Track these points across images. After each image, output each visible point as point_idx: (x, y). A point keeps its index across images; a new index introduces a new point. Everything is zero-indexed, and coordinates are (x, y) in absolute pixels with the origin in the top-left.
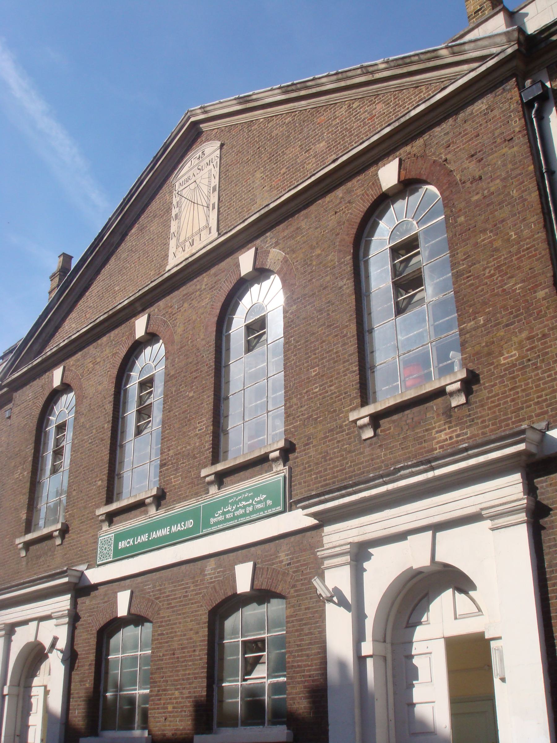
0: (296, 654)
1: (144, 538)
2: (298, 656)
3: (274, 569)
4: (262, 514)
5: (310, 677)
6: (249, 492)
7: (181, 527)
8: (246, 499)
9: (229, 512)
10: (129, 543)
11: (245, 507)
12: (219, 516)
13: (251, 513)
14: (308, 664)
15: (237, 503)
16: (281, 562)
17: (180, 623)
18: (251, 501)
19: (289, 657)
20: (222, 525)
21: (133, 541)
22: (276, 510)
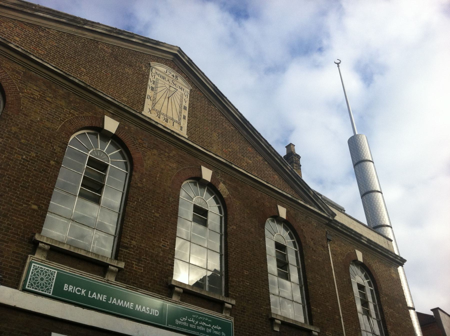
1: (103, 298)
6: (209, 318)
8: (207, 322)
9: (191, 323)
10: (81, 291)
11: (204, 326)
12: (184, 321)
15: (200, 320)
18: (210, 325)
20: (186, 330)
21: (87, 293)
22: (190, 332)
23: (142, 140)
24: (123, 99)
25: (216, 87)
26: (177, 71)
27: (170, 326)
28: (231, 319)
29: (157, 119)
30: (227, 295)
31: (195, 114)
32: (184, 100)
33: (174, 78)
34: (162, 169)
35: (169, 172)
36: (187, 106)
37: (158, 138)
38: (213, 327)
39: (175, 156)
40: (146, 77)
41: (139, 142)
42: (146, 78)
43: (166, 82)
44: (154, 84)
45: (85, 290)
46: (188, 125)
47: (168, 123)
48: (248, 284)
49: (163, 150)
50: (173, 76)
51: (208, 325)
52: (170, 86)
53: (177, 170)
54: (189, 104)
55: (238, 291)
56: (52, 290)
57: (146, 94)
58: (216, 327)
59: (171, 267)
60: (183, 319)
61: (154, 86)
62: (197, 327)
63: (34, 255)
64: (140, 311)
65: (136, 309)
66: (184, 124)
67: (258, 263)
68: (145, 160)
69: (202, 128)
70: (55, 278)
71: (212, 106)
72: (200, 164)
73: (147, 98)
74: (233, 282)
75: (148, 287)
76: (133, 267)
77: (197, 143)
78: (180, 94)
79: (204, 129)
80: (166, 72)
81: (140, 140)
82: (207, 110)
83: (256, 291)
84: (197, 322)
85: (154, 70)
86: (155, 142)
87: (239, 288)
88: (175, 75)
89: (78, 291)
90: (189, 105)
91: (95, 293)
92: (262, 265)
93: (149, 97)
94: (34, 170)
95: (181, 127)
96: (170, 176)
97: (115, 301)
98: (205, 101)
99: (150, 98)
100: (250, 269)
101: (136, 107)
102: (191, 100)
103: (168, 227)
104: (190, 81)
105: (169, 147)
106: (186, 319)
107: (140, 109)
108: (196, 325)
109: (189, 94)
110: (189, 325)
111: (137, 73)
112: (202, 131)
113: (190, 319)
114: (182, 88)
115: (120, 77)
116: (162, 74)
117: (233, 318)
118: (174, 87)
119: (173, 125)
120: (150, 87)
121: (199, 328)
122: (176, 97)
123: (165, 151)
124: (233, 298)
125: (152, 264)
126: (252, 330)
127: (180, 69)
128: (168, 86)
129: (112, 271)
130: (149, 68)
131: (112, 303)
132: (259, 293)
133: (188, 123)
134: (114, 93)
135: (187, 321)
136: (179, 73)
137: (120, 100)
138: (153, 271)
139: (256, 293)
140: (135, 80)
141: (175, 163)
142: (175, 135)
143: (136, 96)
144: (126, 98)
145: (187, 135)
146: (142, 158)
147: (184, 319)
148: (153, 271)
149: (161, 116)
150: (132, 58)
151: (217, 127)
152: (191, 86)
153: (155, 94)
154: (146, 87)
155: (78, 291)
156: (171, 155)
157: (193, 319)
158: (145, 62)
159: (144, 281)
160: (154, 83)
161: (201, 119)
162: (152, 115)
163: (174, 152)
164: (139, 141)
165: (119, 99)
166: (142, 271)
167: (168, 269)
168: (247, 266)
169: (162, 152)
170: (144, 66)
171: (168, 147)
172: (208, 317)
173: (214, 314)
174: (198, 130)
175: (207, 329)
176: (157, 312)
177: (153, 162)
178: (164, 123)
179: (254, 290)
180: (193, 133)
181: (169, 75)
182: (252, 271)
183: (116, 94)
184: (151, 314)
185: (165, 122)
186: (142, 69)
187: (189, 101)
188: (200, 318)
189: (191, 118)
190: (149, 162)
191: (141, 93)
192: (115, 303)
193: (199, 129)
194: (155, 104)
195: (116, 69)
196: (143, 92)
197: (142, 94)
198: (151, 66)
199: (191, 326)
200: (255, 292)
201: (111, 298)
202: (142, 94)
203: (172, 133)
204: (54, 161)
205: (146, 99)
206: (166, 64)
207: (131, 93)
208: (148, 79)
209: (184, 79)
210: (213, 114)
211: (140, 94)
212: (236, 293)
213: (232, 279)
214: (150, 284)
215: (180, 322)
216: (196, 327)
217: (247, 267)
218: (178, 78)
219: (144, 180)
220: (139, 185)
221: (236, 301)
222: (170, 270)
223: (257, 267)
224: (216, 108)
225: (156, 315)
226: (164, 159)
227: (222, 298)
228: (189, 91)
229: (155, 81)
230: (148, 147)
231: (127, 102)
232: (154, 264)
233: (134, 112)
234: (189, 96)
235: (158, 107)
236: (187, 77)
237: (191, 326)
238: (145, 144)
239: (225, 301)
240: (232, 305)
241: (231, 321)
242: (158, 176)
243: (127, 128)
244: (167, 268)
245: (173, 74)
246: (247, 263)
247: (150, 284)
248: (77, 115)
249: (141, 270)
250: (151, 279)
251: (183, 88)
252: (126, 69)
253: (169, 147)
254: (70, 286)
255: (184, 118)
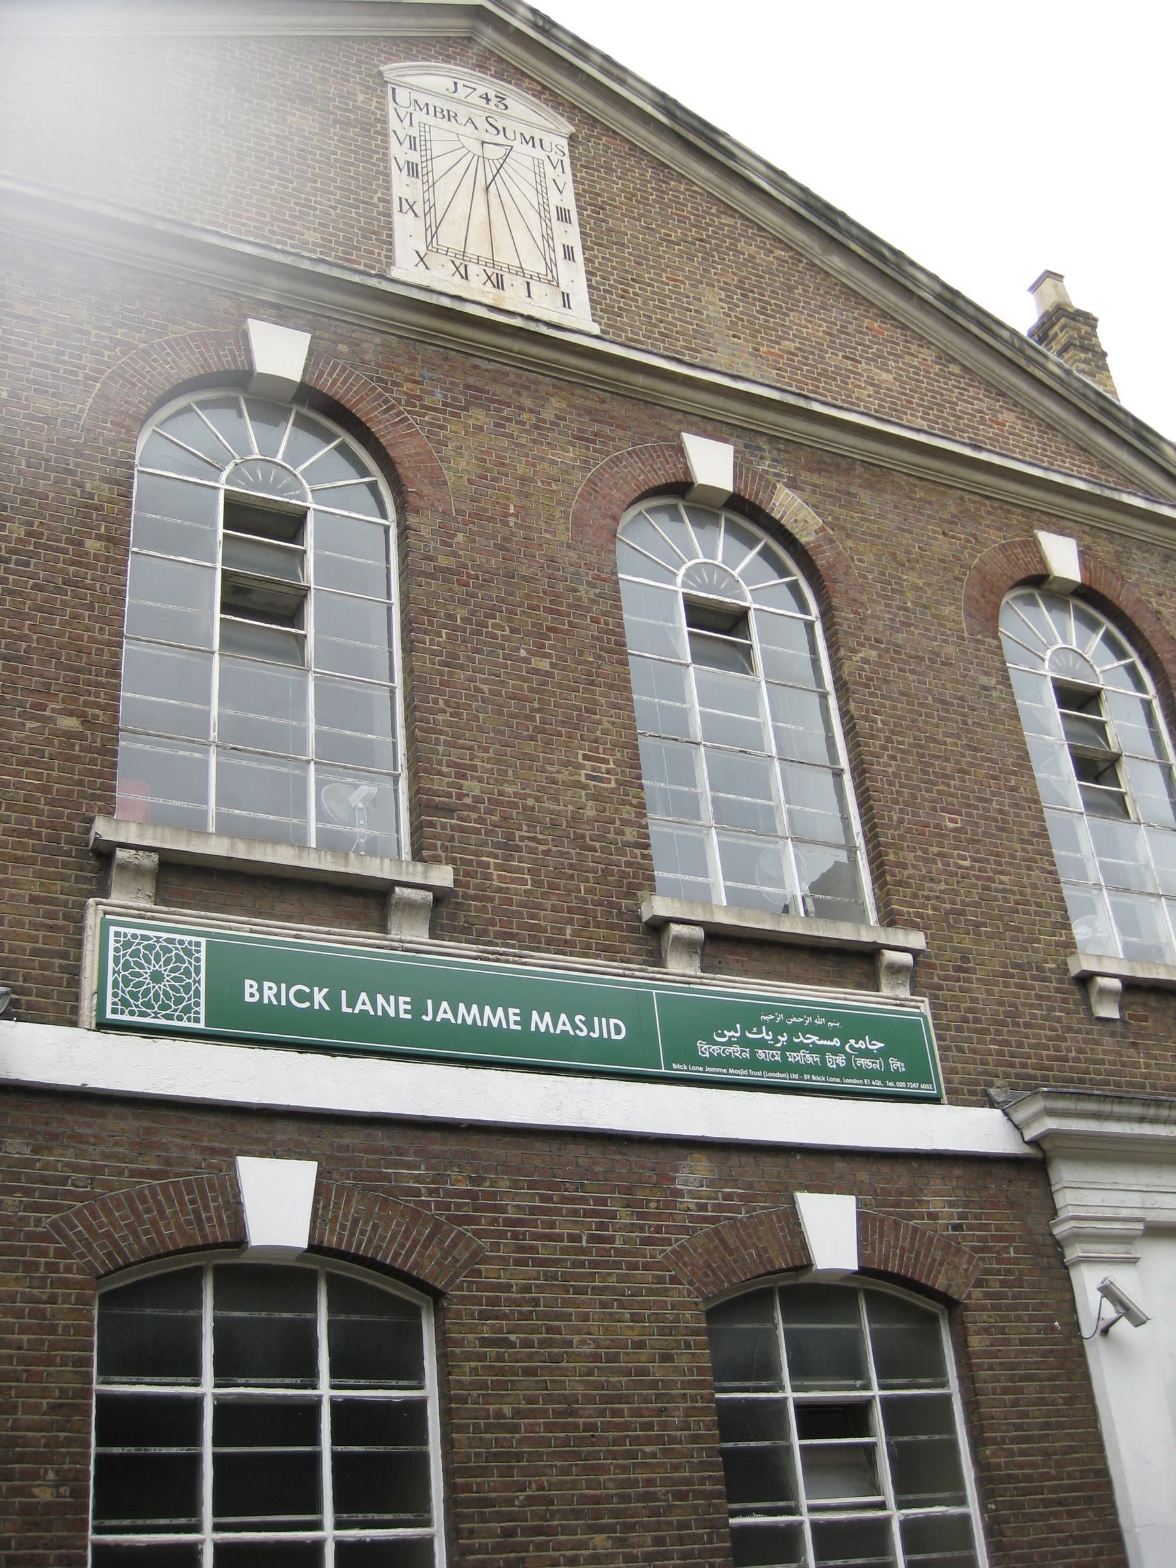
0: (1015, 1447)
1: (398, 1007)
2: (1022, 1453)
3: (915, 1229)
4: (834, 1082)
5: (1060, 1504)
6: (830, 1017)
7: (575, 1027)
8: (824, 1033)
9: (763, 1044)
10: (310, 997)
11: (815, 1049)
12: (729, 1043)
13: (839, 1072)
14: (1048, 1473)
15: (794, 1031)
16: (933, 1216)
17: (585, 1318)
18: (836, 1042)
19: (994, 1454)
23: (415, 382)
24: (305, 237)
25: (675, 102)
26: (499, 76)
27: (678, 1069)
28: (919, 1004)
29: (456, 286)
30: (889, 919)
31: (610, 230)
32: (551, 185)
33: (492, 106)
34: (523, 479)
35: (554, 487)
36: (569, 203)
37: (478, 362)
38: (851, 1047)
39: (564, 419)
40: (379, 128)
41: (406, 394)
42: (376, 132)
43: (462, 130)
44: (415, 150)
45: (325, 990)
46: (588, 280)
47: (508, 292)
48: (967, 863)
49: (509, 405)
50: (488, 100)
51: (829, 1043)
52: (483, 142)
53: (585, 469)
54: (576, 194)
55: (928, 898)
56: (202, 1009)
57: (391, 195)
58: (861, 1045)
59: (638, 852)
60: (725, 1036)
61: (415, 157)
62: (788, 1053)
63: (106, 895)
64: (552, 1031)
65: (533, 1029)
66: (574, 278)
67: (995, 778)
68: (445, 460)
69: (652, 279)
70: (203, 964)
71: (672, 183)
72: (677, 428)
73: (401, 211)
74: (904, 866)
75: (566, 941)
76: (488, 877)
77: (644, 347)
78: (529, 162)
79: (662, 282)
80: (456, 91)
81: (409, 385)
82: (658, 202)
83: (1002, 883)
84: (783, 1039)
85: (402, 95)
86: (471, 380)
87: (930, 885)
88: (491, 95)
89: (300, 996)
90: (577, 200)
91: (363, 996)
92: (1013, 783)
93: (405, 207)
94: (36, 587)
95: (565, 298)
96: (559, 503)
97: (445, 1012)
98: (640, 169)
99: (411, 207)
100: (969, 806)
101: (363, 257)
102: (582, 177)
103: (595, 702)
104: (563, 105)
105: (533, 387)
106: (737, 1032)
107: (379, 261)
108: (783, 1049)
109: (567, 154)
110: (753, 1054)
111: (336, 122)
112: (653, 293)
113: (755, 1030)
114: (532, 138)
115: (272, 155)
116: (440, 104)
117: (926, 999)
118: (500, 139)
119: (529, 296)
120: (401, 164)
121: (792, 1057)
122: (517, 179)
123: (516, 407)
124: (914, 926)
125: (562, 854)
126: (1009, 1032)
127: (508, 62)
128: (476, 148)
129: (410, 906)
130: (381, 91)
131: (438, 1020)
132: (1014, 888)
133: (587, 272)
134: (265, 223)
135: (743, 1042)
136: (510, 82)
137: (293, 246)
138: (571, 877)
139: (1004, 891)
140: (335, 153)
141: (571, 443)
142: (544, 330)
143: (353, 215)
144: (315, 230)
145: (594, 321)
146: (430, 452)
147: (732, 1033)
148: (571, 877)
149: (473, 269)
150: (305, 67)
151: (713, 262)
152: (570, 120)
153: (426, 187)
154: (385, 168)
155: (300, 996)
156: (548, 414)
157: (764, 1027)
158: (360, 73)
159: (542, 923)
160: (413, 146)
161: (639, 245)
162: (433, 273)
163: (554, 402)
164: (405, 389)
165: (289, 241)
166: (529, 887)
167: (629, 864)
168: (952, 795)
169: (506, 412)
170: (358, 88)
171: (527, 388)
172: (823, 1014)
173: (845, 999)
174: (635, 294)
175: (828, 1056)
176: (617, 1028)
177: (477, 458)
178: (489, 295)
179: (994, 882)
180: (620, 308)
181: (469, 99)
182: (975, 812)
183: (273, 225)
184: (595, 1035)
185: (494, 290)
186: (356, 101)
187: (574, 181)
188: (795, 1020)
189: (596, 252)
190: (462, 464)
191: (372, 198)
192: (449, 1020)
193: (640, 289)
194: (437, 228)
195: (252, 125)
196: (376, 192)
197: (375, 200)
198: (387, 82)
199: (761, 1054)
200: (1001, 886)
201: (430, 1002)
202: (375, 200)
203: (532, 326)
204: (99, 537)
205: (398, 219)
206: (448, 58)
207: (331, 207)
208: (386, 135)
209: (534, 99)
210: (685, 214)
211: (366, 203)
212: (924, 907)
213: (896, 854)
214: (569, 929)
215: (715, 1047)
216: (784, 1057)
217: (950, 799)
218: (508, 102)
219: (460, 537)
220: (443, 561)
221: (926, 934)
222: (639, 864)
223: (993, 794)
224: (695, 188)
225: (614, 1037)
226: (522, 441)
227: (869, 932)
228: (564, 143)
229: (417, 135)
230: (445, 404)
231: (323, 246)
232: (568, 853)
233: (356, 279)
234: (567, 162)
235: (450, 237)
236: (544, 87)
237: (761, 1054)
238: (432, 394)
239: (882, 940)
240: (915, 953)
241: (918, 1011)
242: (512, 511)
243: (346, 347)
244: (623, 859)
245: (482, 90)
246: (948, 786)
247: (569, 929)
248: (142, 346)
249: (523, 882)
250: (570, 910)
251: (538, 135)
252: (288, 117)
253: (533, 387)
254: (266, 984)
255: (569, 254)
